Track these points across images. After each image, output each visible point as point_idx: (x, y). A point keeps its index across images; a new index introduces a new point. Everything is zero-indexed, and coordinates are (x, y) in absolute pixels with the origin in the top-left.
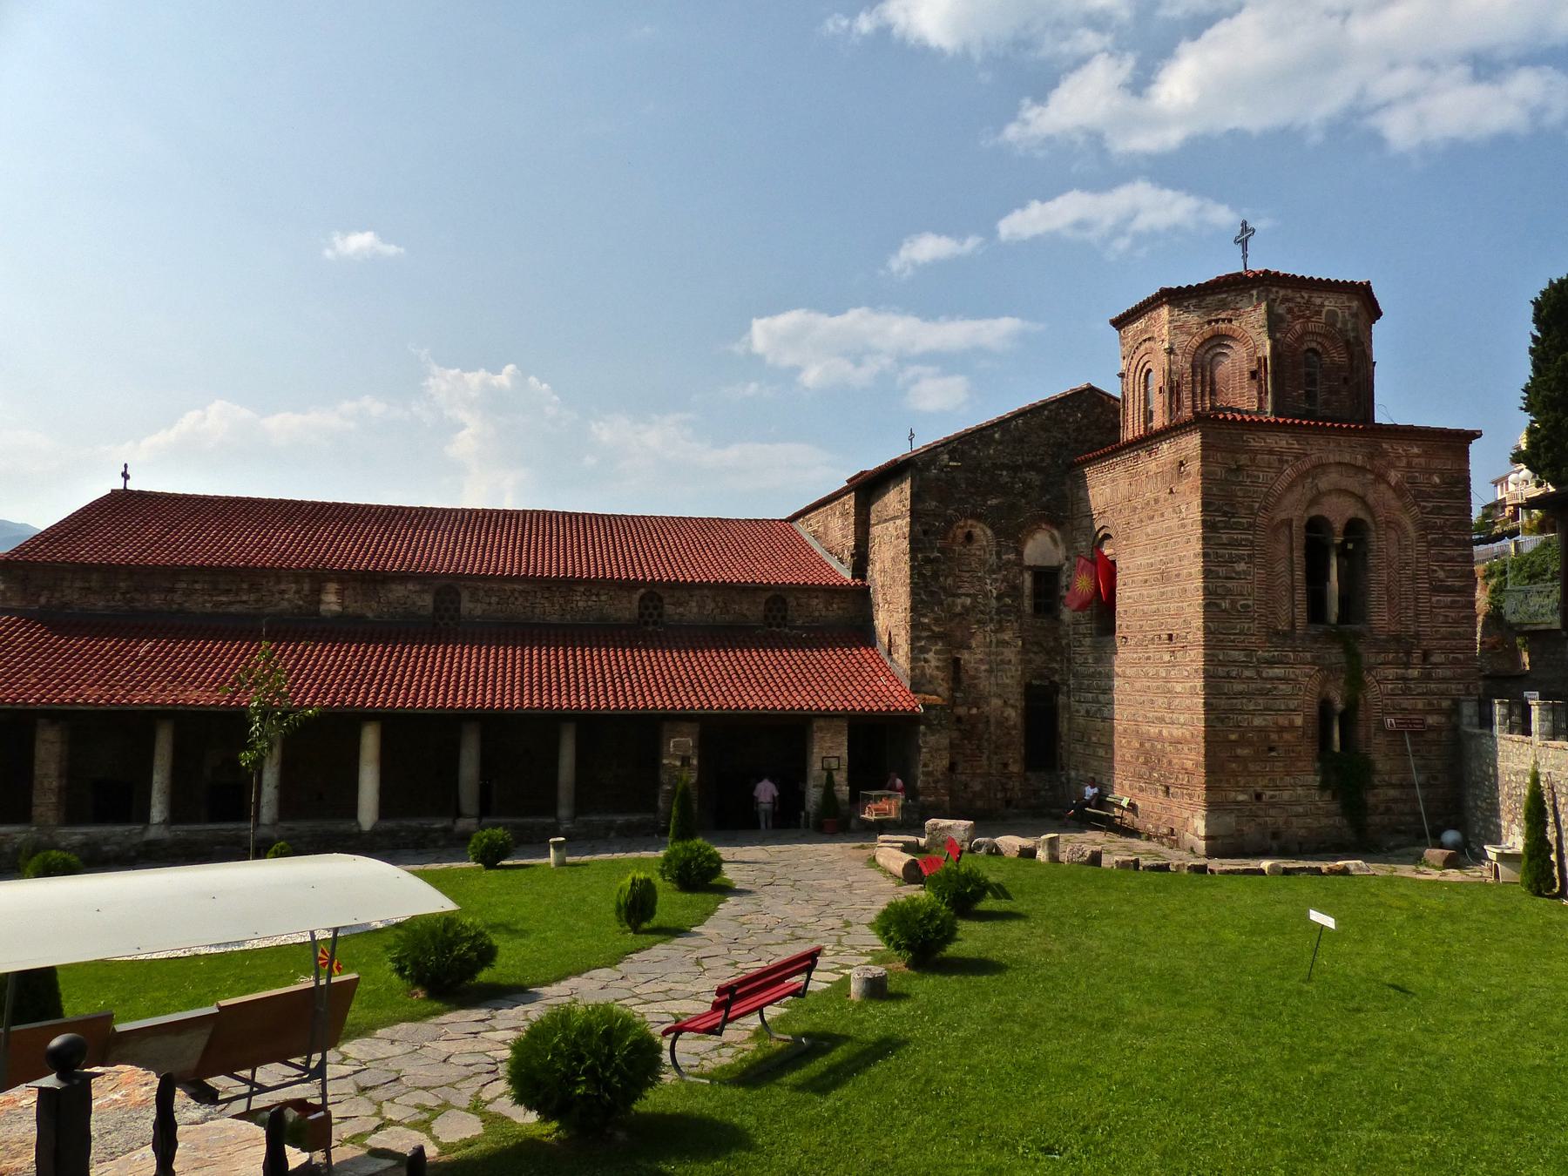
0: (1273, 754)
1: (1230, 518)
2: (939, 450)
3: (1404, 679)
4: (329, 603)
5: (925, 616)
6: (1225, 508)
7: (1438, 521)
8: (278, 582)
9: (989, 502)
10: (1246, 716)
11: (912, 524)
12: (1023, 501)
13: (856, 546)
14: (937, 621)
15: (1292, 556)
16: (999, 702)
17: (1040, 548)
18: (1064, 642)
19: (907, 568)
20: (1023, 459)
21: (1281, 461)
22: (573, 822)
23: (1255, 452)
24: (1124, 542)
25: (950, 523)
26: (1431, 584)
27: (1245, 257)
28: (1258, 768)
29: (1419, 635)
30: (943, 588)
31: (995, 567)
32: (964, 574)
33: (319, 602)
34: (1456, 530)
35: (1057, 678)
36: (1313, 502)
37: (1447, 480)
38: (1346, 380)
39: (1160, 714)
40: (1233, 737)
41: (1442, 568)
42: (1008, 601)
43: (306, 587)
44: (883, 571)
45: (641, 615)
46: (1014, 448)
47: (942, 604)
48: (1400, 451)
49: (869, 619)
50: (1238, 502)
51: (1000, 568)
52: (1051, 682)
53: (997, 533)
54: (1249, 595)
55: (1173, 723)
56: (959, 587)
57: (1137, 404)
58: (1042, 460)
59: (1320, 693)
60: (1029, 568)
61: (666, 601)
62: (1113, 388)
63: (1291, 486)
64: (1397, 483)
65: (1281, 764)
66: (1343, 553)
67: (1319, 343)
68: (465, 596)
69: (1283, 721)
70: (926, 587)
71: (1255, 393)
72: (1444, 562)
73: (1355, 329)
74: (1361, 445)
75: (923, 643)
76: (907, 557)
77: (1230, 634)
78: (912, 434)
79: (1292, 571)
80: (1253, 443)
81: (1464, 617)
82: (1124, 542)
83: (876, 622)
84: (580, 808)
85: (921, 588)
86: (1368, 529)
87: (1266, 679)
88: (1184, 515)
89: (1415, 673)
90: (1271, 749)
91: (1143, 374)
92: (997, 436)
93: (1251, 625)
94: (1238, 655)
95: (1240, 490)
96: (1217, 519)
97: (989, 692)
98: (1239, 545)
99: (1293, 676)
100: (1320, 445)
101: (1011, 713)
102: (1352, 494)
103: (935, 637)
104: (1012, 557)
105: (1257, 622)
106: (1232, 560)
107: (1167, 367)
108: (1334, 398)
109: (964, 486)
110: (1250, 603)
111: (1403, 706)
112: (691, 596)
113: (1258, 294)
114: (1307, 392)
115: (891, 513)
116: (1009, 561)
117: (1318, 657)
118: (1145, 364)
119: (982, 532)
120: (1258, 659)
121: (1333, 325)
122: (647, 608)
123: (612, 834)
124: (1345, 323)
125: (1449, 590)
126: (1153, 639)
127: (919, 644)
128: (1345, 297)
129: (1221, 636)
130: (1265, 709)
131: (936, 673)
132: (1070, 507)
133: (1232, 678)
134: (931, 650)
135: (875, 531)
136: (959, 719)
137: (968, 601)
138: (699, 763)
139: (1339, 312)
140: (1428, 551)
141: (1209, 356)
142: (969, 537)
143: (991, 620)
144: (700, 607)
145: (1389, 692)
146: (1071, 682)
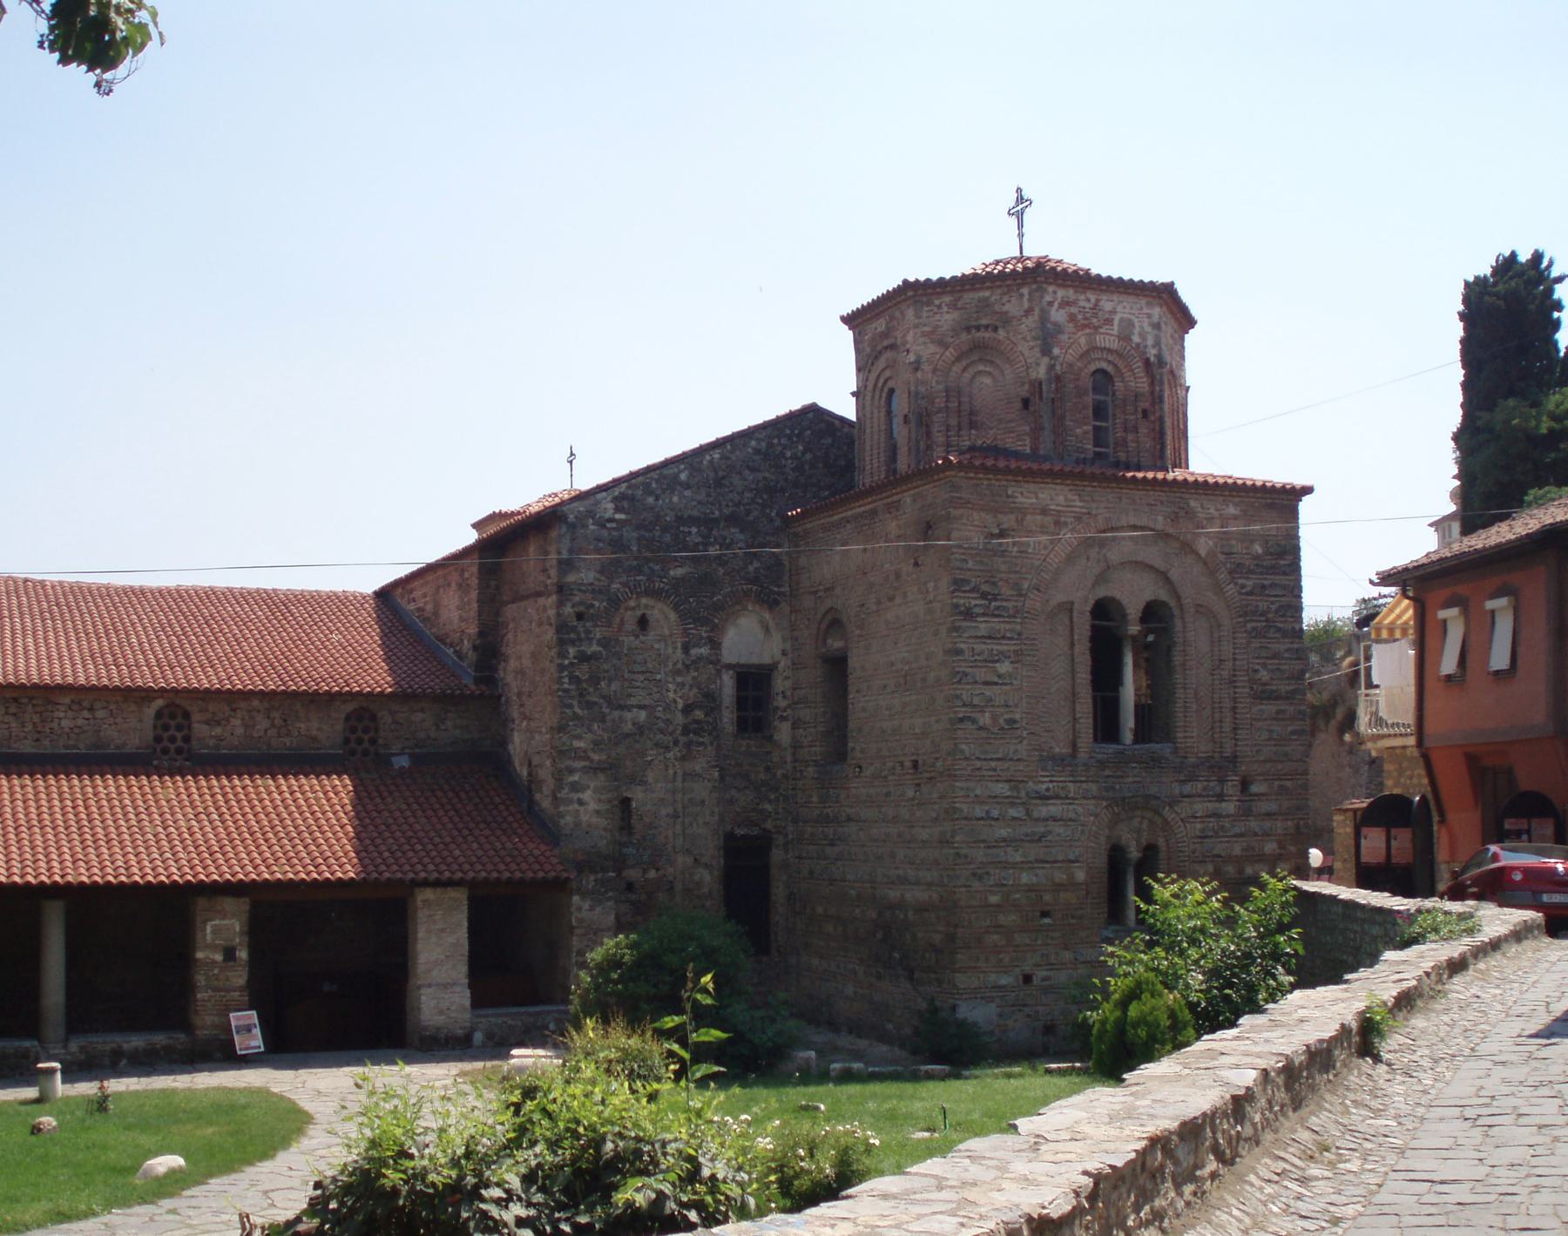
0: (1047, 921)
1: (990, 601)
2: (599, 496)
3: (1216, 815)
5: (579, 737)
6: (985, 588)
7: (1260, 604)
9: (672, 573)
10: (1011, 871)
12: (721, 571)
13: (481, 634)
14: (596, 743)
15: (1072, 655)
16: (689, 860)
18: (779, 773)
19: (553, 669)
20: (720, 510)
21: (1057, 523)
22: (65, 1047)
23: (1022, 512)
24: (858, 632)
25: (615, 602)
26: (1252, 689)
27: (1021, 235)
28: (1027, 941)
29: (1236, 757)
30: (607, 699)
31: (680, 666)
32: (635, 676)
34: (1283, 616)
35: (769, 825)
36: (1101, 579)
37: (1272, 550)
38: (1145, 414)
39: (901, 872)
40: (994, 899)
41: (1264, 666)
42: (699, 714)
44: (520, 672)
45: (158, 739)
46: (708, 495)
47: (603, 720)
48: (1212, 511)
49: (504, 742)
50: (1001, 579)
51: (687, 667)
52: (764, 830)
53: (683, 616)
54: (1016, 706)
55: (918, 883)
56: (630, 695)
57: (876, 437)
58: (748, 512)
59: (1109, 837)
60: (729, 667)
61: (196, 717)
62: (846, 408)
63: (1071, 559)
64: (1208, 554)
65: (1057, 934)
66: (1141, 647)
67: (1109, 362)
69: (1060, 876)
70: (581, 695)
71: (1027, 428)
72: (1268, 658)
73: (1157, 344)
74: (1162, 503)
75: (576, 777)
76: (553, 652)
77: (991, 759)
78: (572, 454)
79: (1073, 671)
80: (1020, 499)
81: (1293, 732)
82: (858, 632)
83: (511, 747)
84: (77, 1022)
85: (572, 698)
86: (1172, 616)
87: (1038, 820)
88: (931, 597)
89: (1229, 807)
90: (1044, 914)
91: (884, 395)
92: (683, 476)
93: (1019, 747)
94: (1002, 789)
95: (1004, 562)
96: (974, 602)
97: (674, 847)
98: (1003, 638)
99: (1072, 815)
101: (707, 878)
102: (1151, 567)
103: (595, 769)
104: (704, 651)
105: (1025, 742)
106: (993, 659)
107: (913, 388)
108: (1130, 437)
109: (635, 549)
110: (1018, 717)
111: (1215, 852)
112: (234, 710)
113: (1030, 294)
114: (1096, 429)
116: (700, 658)
117: (1107, 789)
118: (886, 381)
119: (663, 616)
120: (1027, 793)
121: (1128, 339)
122: (166, 728)
123: (124, 1062)
124: (1143, 335)
125: (1273, 697)
126: (894, 768)
127: (571, 779)
128: (1143, 301)
129: (978, 764)
130: (1037, 861)
131: (595, 820)
132: (786, 578)
133: (993, 819)
134: (589, 787)
135: (510, 611)
136: (630, 887)
137: (643, 715)
138: (252, 954)
139: (1136, 320)
141: (967, 375)
142: (643, 623)
143: (676, 743)
144: (246, 727)
145: (1198, 834)
146: (790, 829)
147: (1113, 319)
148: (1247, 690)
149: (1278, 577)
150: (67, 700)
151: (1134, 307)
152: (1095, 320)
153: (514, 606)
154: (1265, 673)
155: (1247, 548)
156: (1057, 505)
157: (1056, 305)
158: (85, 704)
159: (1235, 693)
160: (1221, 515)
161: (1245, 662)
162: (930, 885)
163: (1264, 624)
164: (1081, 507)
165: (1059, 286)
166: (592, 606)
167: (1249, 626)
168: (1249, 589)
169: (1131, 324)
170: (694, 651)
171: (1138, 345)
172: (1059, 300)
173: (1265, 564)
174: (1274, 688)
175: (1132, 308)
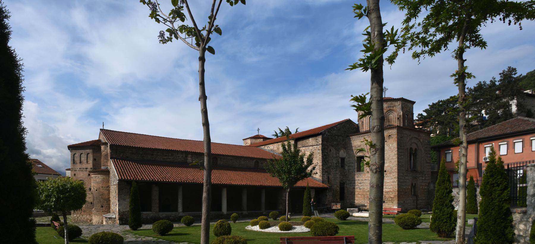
0: (406, 194)
4: (189, 160)
8: (178, 154)
11: (322, 147)
17: (342, 153)
33: (187, 159)
40: (401, 190)
43: (184, 155)
68: (219, 159)
76: (321, 154)
89: (424, 178)
92: (335, 129)
115: (311, 144)
125: (428, 163)
130: (406, 185)
142: (330, 150)
150: (243, 159)
153: (304, 148)
158: (245, 160)
162: (390, 189)
166: (325, 147)
170: (337, 155)
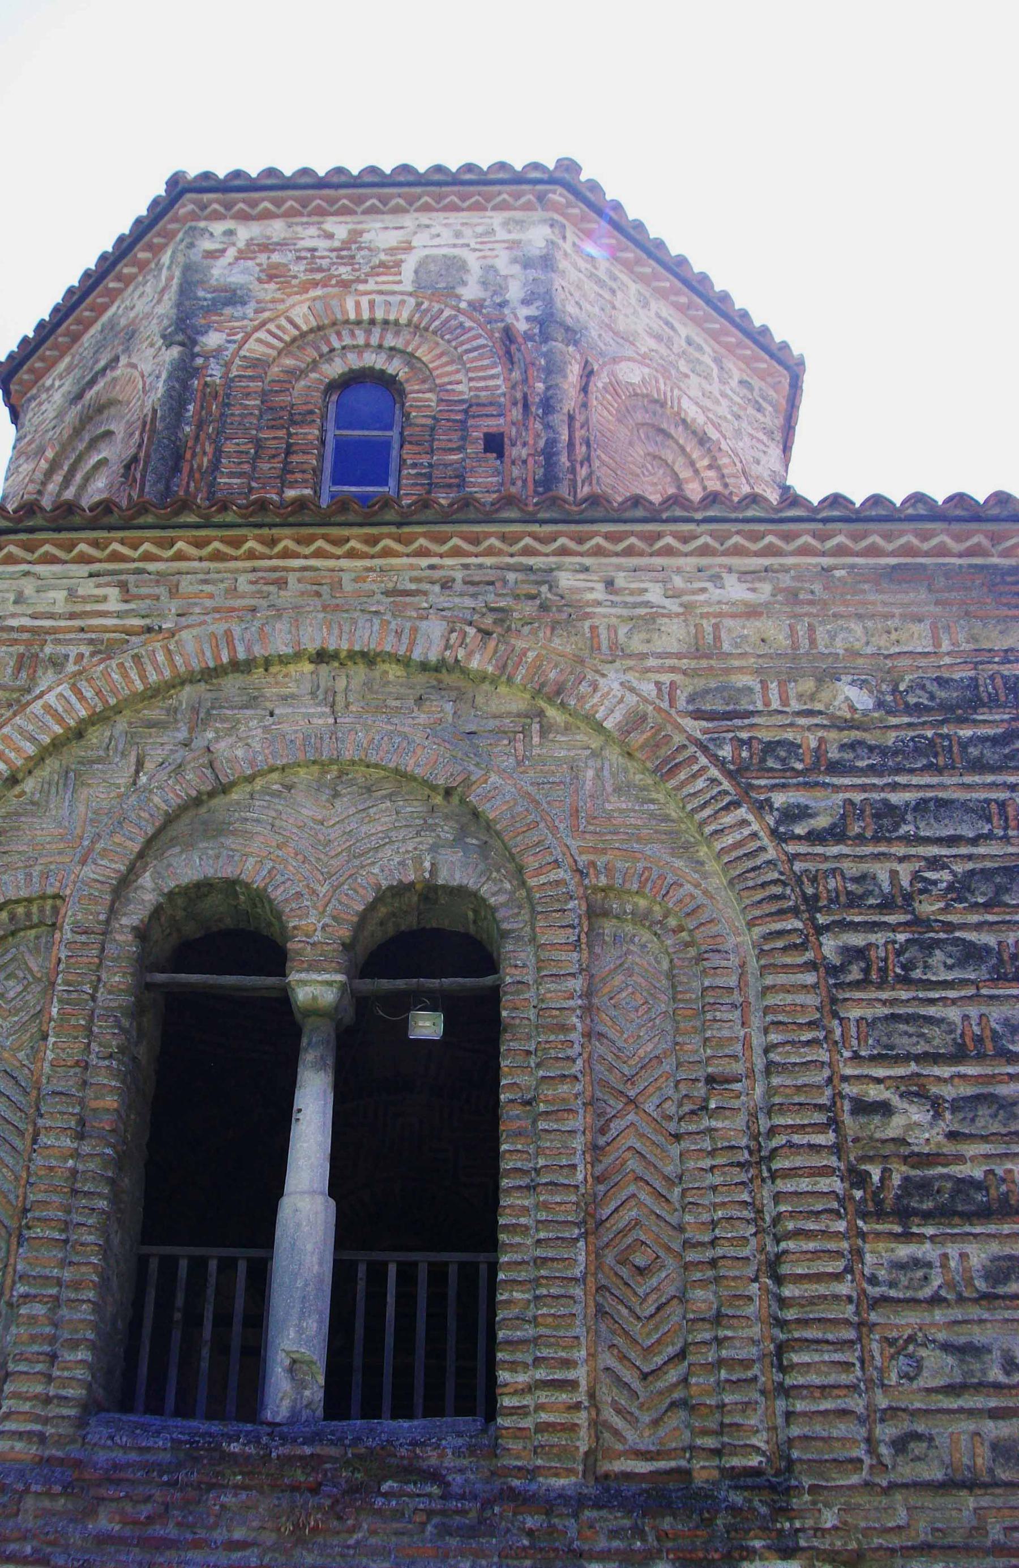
7: (882, 872)
26: (857, 1178)
64: (636, 721)
100: (233, 591)
140: (833, 1006)
147: (398, 264)
148: (836, 1184)
149: (947, 780)
151: (468, 232)
152: (342, 270)
154: (918, 1114)
155: (812, 698)
156: (34, 617)
157: (231, 253)
159: (778, 1197)
160: (688, 607)
161: (819, 1077)
163: (901, 937)
164: (119, 615)
165: (244, 217)
167: (830, 946)
168: (822, 822)
169: (455, 266)
171: (476, 306)
172: (241, 244)
173: (890, 738)
174: (978, 1173)
175: (458, 235)
